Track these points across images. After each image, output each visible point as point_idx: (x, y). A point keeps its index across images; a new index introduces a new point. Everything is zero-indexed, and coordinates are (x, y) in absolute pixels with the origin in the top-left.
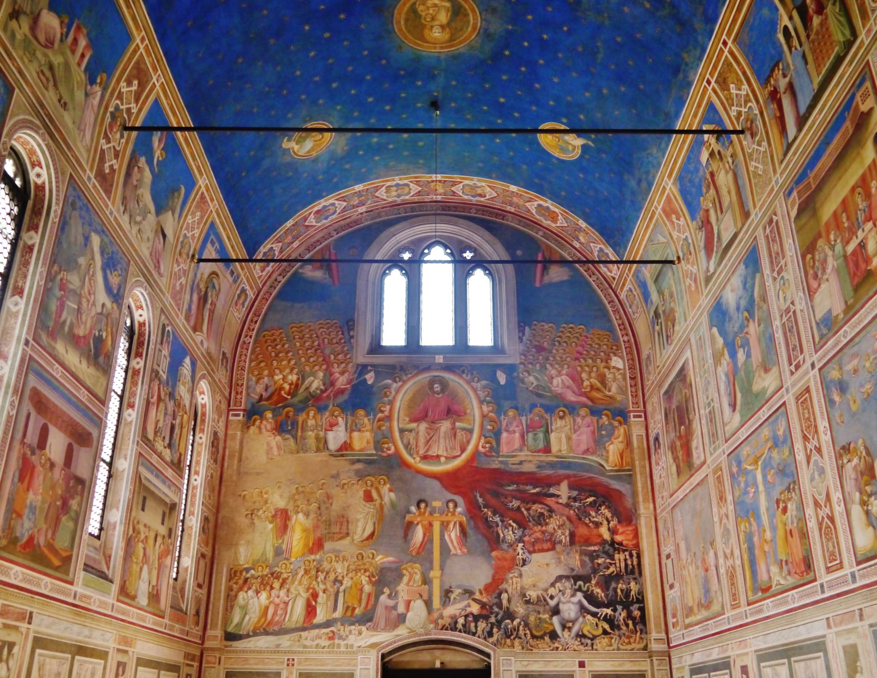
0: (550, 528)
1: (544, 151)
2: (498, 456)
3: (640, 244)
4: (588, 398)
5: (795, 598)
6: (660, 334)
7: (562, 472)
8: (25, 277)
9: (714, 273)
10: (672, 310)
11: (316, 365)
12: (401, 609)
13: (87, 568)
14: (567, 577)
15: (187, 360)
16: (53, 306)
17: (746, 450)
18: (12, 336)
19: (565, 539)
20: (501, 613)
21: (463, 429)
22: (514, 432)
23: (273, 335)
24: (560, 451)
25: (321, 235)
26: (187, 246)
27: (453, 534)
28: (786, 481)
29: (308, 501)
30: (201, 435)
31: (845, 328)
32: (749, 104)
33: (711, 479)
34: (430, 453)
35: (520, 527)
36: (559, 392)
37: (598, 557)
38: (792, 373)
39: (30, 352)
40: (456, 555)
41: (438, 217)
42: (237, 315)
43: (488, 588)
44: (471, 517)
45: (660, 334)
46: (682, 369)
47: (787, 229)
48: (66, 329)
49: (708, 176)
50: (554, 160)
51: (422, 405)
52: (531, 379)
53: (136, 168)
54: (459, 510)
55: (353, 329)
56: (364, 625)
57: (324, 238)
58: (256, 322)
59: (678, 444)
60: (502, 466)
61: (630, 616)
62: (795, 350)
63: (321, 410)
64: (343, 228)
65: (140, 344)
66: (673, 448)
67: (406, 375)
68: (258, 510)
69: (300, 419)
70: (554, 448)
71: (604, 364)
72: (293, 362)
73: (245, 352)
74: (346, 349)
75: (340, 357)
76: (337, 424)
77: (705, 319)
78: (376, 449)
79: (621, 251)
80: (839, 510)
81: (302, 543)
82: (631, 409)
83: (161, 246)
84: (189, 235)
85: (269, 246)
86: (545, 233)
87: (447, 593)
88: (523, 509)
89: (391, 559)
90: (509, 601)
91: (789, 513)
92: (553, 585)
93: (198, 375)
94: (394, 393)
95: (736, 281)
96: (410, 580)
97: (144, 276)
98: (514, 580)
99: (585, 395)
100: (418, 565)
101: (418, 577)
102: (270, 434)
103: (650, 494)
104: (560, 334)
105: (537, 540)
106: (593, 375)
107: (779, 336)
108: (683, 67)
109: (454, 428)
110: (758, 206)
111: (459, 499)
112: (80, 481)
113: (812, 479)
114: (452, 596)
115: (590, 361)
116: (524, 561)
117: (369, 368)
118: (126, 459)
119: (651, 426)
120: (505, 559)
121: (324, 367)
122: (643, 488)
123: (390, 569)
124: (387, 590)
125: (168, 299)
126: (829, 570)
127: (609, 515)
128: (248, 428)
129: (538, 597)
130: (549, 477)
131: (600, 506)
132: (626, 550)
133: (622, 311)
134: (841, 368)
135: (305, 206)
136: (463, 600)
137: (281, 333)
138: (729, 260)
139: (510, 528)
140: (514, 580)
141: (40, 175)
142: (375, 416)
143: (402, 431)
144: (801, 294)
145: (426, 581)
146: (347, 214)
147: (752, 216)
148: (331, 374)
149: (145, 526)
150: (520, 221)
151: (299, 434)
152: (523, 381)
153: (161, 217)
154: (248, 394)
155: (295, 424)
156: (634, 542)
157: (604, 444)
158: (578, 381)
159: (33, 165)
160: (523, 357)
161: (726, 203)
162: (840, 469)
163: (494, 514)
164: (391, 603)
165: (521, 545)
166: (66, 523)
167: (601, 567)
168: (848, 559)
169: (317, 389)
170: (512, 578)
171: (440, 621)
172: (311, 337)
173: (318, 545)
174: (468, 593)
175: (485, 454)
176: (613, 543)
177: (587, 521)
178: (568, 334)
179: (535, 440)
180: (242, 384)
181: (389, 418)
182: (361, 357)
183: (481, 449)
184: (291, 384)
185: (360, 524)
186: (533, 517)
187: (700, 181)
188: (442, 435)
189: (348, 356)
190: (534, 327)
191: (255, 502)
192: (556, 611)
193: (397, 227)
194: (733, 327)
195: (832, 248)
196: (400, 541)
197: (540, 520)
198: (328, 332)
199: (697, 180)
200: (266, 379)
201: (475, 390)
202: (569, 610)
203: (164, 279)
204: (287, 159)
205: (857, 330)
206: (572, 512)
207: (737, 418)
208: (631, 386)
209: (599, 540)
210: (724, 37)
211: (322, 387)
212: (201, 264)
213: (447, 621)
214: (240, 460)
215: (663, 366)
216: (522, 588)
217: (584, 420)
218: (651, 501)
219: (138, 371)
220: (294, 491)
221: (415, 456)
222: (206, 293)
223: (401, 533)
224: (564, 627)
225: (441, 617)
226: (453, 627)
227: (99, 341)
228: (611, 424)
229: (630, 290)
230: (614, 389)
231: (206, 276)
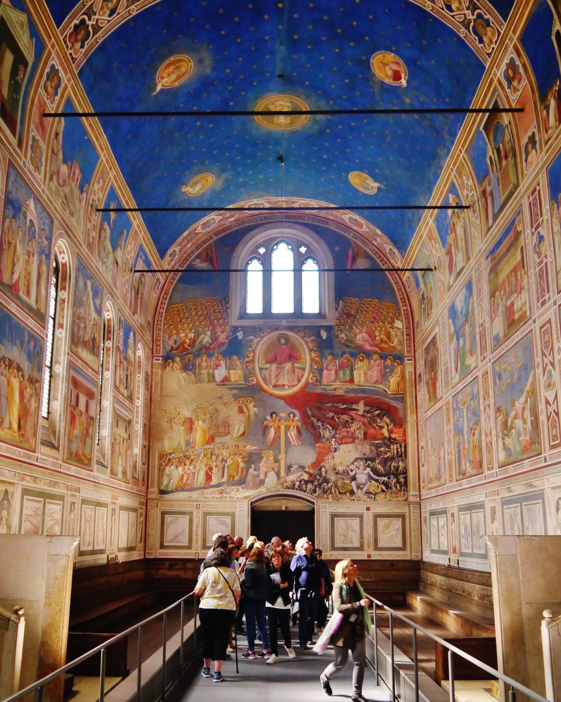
0: (352, 430)
1: (353, 187)
2: (321, 385)
3: (414, 251)
4: (379, 348)
6: (424, 310)
7: (361, 395)
8: (63, 317)
9: (452, 286)
10: (431, 299)
11: (205, 327)
12: (262, 477)
14: (361, 459)
15: (132, 334)
16: (76, 330)
17: (460, 397)
18: (61, 351)
19: (361, 436)
20: (321, 479)
21: (299, 368)
22: (331, 370)
23: (177, 307)
24: (360, 382)
25: (205, 237)
26: (128, 264)
27: (293, 433)
28: (476, 419)
29: (204, 413)
30: (139, 375)
31: (503, 346)
32: (473, 192)
33: (444, 408)
34: (278, 383)
35: (333, 429)
36: (361, 344)
37: (381, 447)
38: (482, 361)
39: (70, 358)
40: (294, 445)
41: (283, 224)
42: (155, 295)
43: (313, 465)
44: (304, 423)
45: (424, 310)
46: (434, 338)
47: (485, 276)
48: (81, 339)
49: (452, 225)
50: (360, 193)
51: (273, 353)
52: (343, 335)
53: (103, 231)
54: (296, 418)
55: (229, 303)
56: (240, 486)
57: (208, 240)
58: (166, 299)
59: (430, 382)
60: (323, 392)
62: (483, 348)
63: (210, 356)
64: (219, 232)
65: (109, 332)
66: (427, 384)
67: (263, 333)
68: (174, 418)
70: (356, 380)
71: (390, 325)
72: (191, 325)
73: (160, 318)
74: (224, 316)
75: (221, 321)
76: (220, 365)
77: (446, 311)
78: (244, 381)
79: (403, 253)
81: (202, 438)
82: (406, 355)
83: (115, 271)
84: (129, 257)
85: (173, 249)
86: (354, 234)
87: (289, 468)
88: (336, 418)
89: (255, 448)
90: (326, 472)
91: (475, 436)
92: (353, 463)
93: (137, 340)
94: (255, 345)
95: (461, 296)
96: (267, 460)
97: (110, 293)
98: (330, 460)
99: (377, 346)
100: (271, 451)
101: (272, 458)
102: (178, 371)
103: (415, 409)
104: (362, 305)
105: (344, 437)
106: (383, 332)
107: (478, 337)
108: (438, 157)
109: (293, 367)
110: (474, 256)
111: (296, 412)
113: (485, 421)
114: (292, 470)
115: (381, 323)
116: (336, 449)
117: (240, 329)
118: (107, 400)
119: (417, 366)
120: (324, 448)
121: (211, 328)
122: (410, 405)
124: (253, 466)
125: (121, 301)
127: (388, 422)
128: (165, 368)
129: (343, 470)
130: (352, 398)
131: (383, 416)
132: (398, 443)
133: (403, 290)
134: (500, 367)
135: (195, 221)
136: (298, 472)
137: (182, 306)
138: (460, 281)
139: (328, 430)
140: (330, 460)
141: (65, 258)
142: (244, 360)
143: (261, 369)
144: (488, 318)
145: (276, 461)
146: (222, 223)
147: (471, 261)
148: (216, 333)
149: (119, 435)
150: (338, 226)
151: (197, 371)
152: (337, 337)
153: (115, 253)
154: (164, 346)
155: (194, 365)
156: (403, 438)
157: (388, 377)
158: (372, 336)
159: (60, 253)
160: (338, 321)
161: (460, 246)
163: (318, 421)
164: (256, 473)
165: (334, 440)
167: (382, 453)
169: (207, 342)
170: (328, 459)
171: (285, 484)
172: (202, 309)
173: (212, 439)
174: (302, 467)
175: (312, 384)
176: (390, 439)
177: (375, 425)
178: (368, 305)
179: (344, 375)
180: (160, 340)
181: (253, 361)
182: (234, 321)
183: (310, 381)
184: (190, 340)
185: (236, 427)
186: (341, 423)
187: (447, 226)
188: (286, 372)
189: (226, 321)
190: (345, 301)
191: (172, 414)
193: (257, 231)
194: (460, 322)
195: (502, 299)
196: (261, 437)
197: (346, 424)
198: (212, 305)
199: (446, 224)
200: (175, 336)
201: (307, 343)
203: (119, 290)
204: (185, 197)
205: (508, 349)
206: (366, 420)
208: (407, 340)
209: (382, 437)
210: (460, 147)
211: (210, 341)
212: (136, 273)
213: (289, 484)
214: (162, 388)
215: (425, 332)
216: (334, 465)
217: (376, 363)
218: (415, 413)
219: (110, 349)
220: (195, 407)
221: (269, 385)
222: (138, 288)
223: (261, 432)
225: (286, 481)
227: (94, 339)
228: (392, 365)
229: (408, 277)
230: (396, 342)
231: (138, 278)
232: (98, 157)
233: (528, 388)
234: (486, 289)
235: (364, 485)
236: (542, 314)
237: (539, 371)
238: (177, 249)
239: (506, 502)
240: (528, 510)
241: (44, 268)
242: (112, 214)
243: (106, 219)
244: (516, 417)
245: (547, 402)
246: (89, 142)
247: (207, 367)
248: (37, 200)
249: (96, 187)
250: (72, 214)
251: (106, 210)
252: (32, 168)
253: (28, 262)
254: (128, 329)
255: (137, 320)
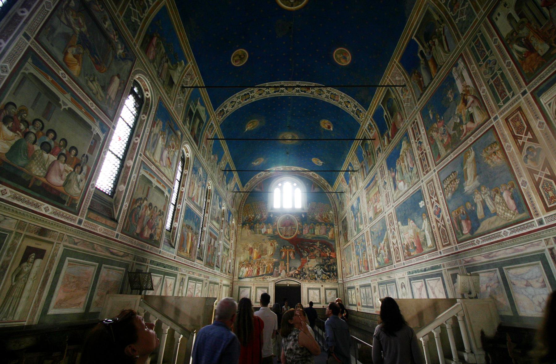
0: (315, 253)
5: (366, 275)
7: (317, 239)
13: (217, 266)
14: (319, 265)
19: (318, 256)
27: (292, 254)
42: (240, 201)
43: (300, 267)
46: (346, 217)
47: (365, 195)
57: (260, 181)
61: (334, 274)
62: (366, 222)
63: (260, 224)
66: (344, 235)
69: (255, 226)
70: (316, 233)
77: (350, 208)
80: (373, 258)
101: (283, 264)
105: (312, 256)
107: (363, 218)
109: (292, 228)
111: (293, 246)
112: (215, 248)
123: (277, 262)
126: (371, 270)
141: (210, 188)
143: (279, 229)
145: (285, 265)
155: (254, 227)
162: (373, 249)
164: (277, 270)
166: (214, 257)
168: (374, 268)
174: (295, 268)
176: (330, 256)
181: (276, 226)
192: (316, 273)
197: (313, 251)
202: (319, 273)
204: (252, 166)
207: (356, 233)
213: (290, 275)
217: (323, 226)
224: (318, 277)
226: (292, 276)
227: (218, 217)
232: (224, 152)
233: (385, 238)
234: (365, 200)
235: (320, 276)
236: (388, 210)
237: (389, 232)
238: (249, 184)
239: (380, 284)
240: (390, 288)
241: (203, 191)
242: (227, 172)
243: (225, 174)
244: (381, 249)
245: (393, 244)
246: (222, 148)
247: (259, 228)
248: (203, 168)
249: (223, 163)
250: (214, 172)
251: (225, 171)
252: (202, 157)
253: (198, 190)
254: (230, 213)
255: (233, 210)
